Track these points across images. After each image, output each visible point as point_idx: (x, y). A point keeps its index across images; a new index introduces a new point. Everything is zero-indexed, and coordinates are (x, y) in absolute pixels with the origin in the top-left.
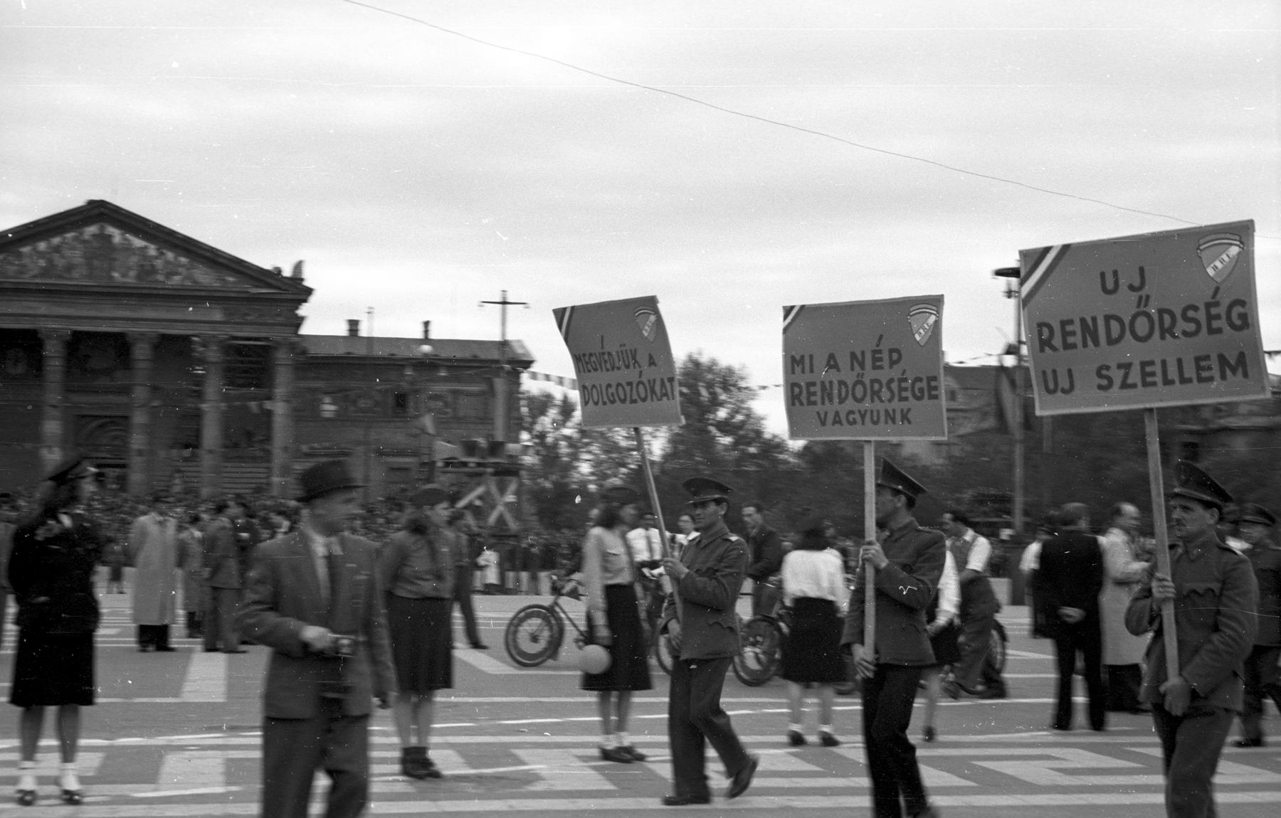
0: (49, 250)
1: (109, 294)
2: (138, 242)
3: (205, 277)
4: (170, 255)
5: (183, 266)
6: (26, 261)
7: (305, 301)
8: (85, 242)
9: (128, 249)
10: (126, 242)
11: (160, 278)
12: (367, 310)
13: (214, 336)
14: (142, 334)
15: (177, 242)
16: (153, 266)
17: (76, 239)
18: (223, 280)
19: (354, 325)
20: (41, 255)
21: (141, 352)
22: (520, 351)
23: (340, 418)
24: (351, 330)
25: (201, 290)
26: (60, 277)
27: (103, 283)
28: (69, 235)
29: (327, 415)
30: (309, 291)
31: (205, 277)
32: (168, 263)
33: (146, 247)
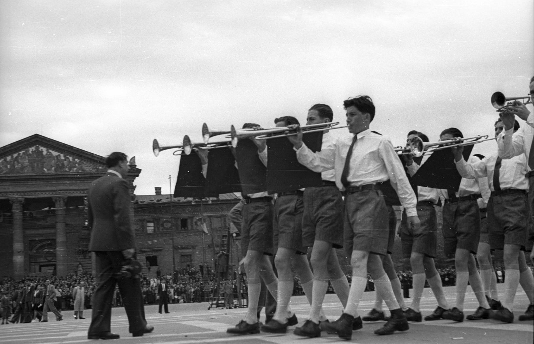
1: (43, 179)
2: (55, 154)
3: (88, 168)
4: (71, 159)
5: (77, 163)
7: (138, 176)
9: (50, 156)
10: (48, 154)
11: (67, 170)
12: (169, 177)
14: (59, 197)
15: (75, 152)
16: (63, 164)
17: (24, 153)
18: (98, 169)
19: (158, 190)
23: (155, 234)
24: (156, 192)
25: (86, 174)
26: (18, 172)
27: (41, 174)
28: (21, 152)
29: (149, 232)
30: (139, 171)
31: (88, 168)
32: (70, 162)
33: (59, 155)
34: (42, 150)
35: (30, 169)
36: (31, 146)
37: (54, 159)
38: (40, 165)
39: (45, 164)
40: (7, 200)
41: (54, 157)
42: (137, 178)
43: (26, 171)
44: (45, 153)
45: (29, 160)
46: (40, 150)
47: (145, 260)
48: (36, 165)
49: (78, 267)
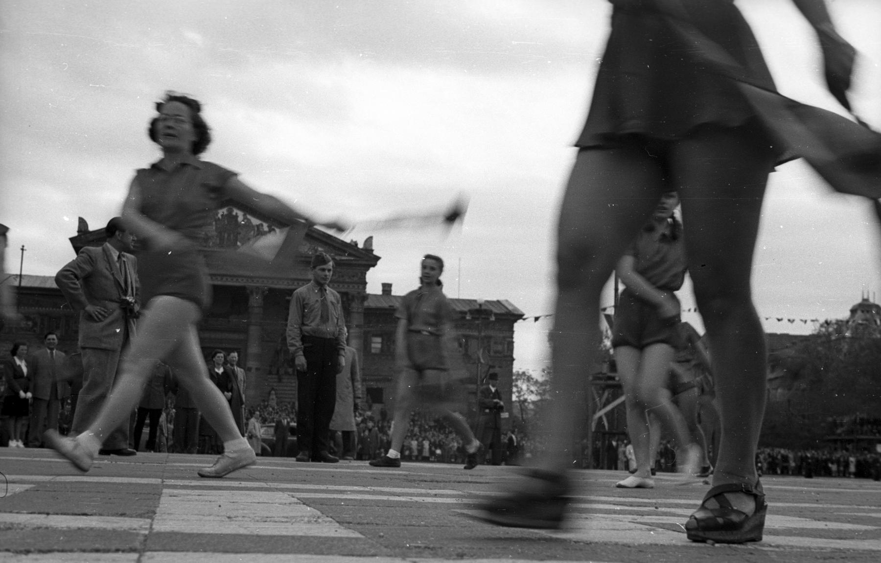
2: (255, 221)
7: (374, 266)
9: (249, 225)
14: (257, 288)
18: (316, 251)
21: (256, 300)
22: (510, 308)
24: (384, 291)
29: (373, 351)
30: (378, 258)
34: (236, 214)
35: (218, 241)
36: (222, 207)
37: (254, 230)
38: (232, 236)
39: (239, 237)
41: (253, 226)
42: (372, 269)
43: (211, 243)
44: (240, 218)
45: (217, 228)
46: (234, 213)
47: (366, 393)
48: (226, 236)
49: (269, 394)
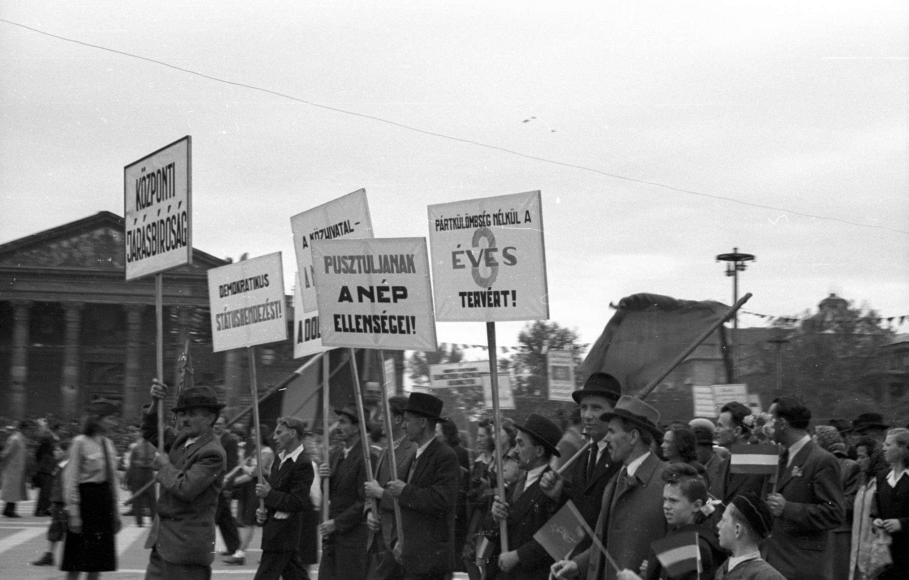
0: (70, 247)
6: (54, 254)
8: (95, 240)
13: (184, 307)
14: (134, 305)
17: (88, 239)
20: (64, 249)
26: (78, 265)
40: (58, 304)
